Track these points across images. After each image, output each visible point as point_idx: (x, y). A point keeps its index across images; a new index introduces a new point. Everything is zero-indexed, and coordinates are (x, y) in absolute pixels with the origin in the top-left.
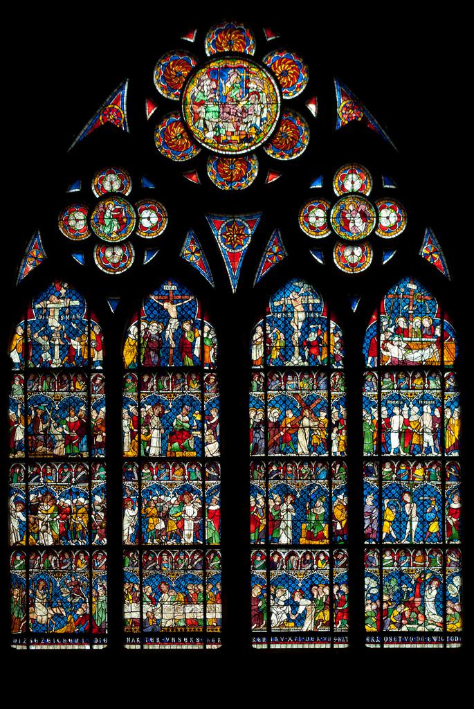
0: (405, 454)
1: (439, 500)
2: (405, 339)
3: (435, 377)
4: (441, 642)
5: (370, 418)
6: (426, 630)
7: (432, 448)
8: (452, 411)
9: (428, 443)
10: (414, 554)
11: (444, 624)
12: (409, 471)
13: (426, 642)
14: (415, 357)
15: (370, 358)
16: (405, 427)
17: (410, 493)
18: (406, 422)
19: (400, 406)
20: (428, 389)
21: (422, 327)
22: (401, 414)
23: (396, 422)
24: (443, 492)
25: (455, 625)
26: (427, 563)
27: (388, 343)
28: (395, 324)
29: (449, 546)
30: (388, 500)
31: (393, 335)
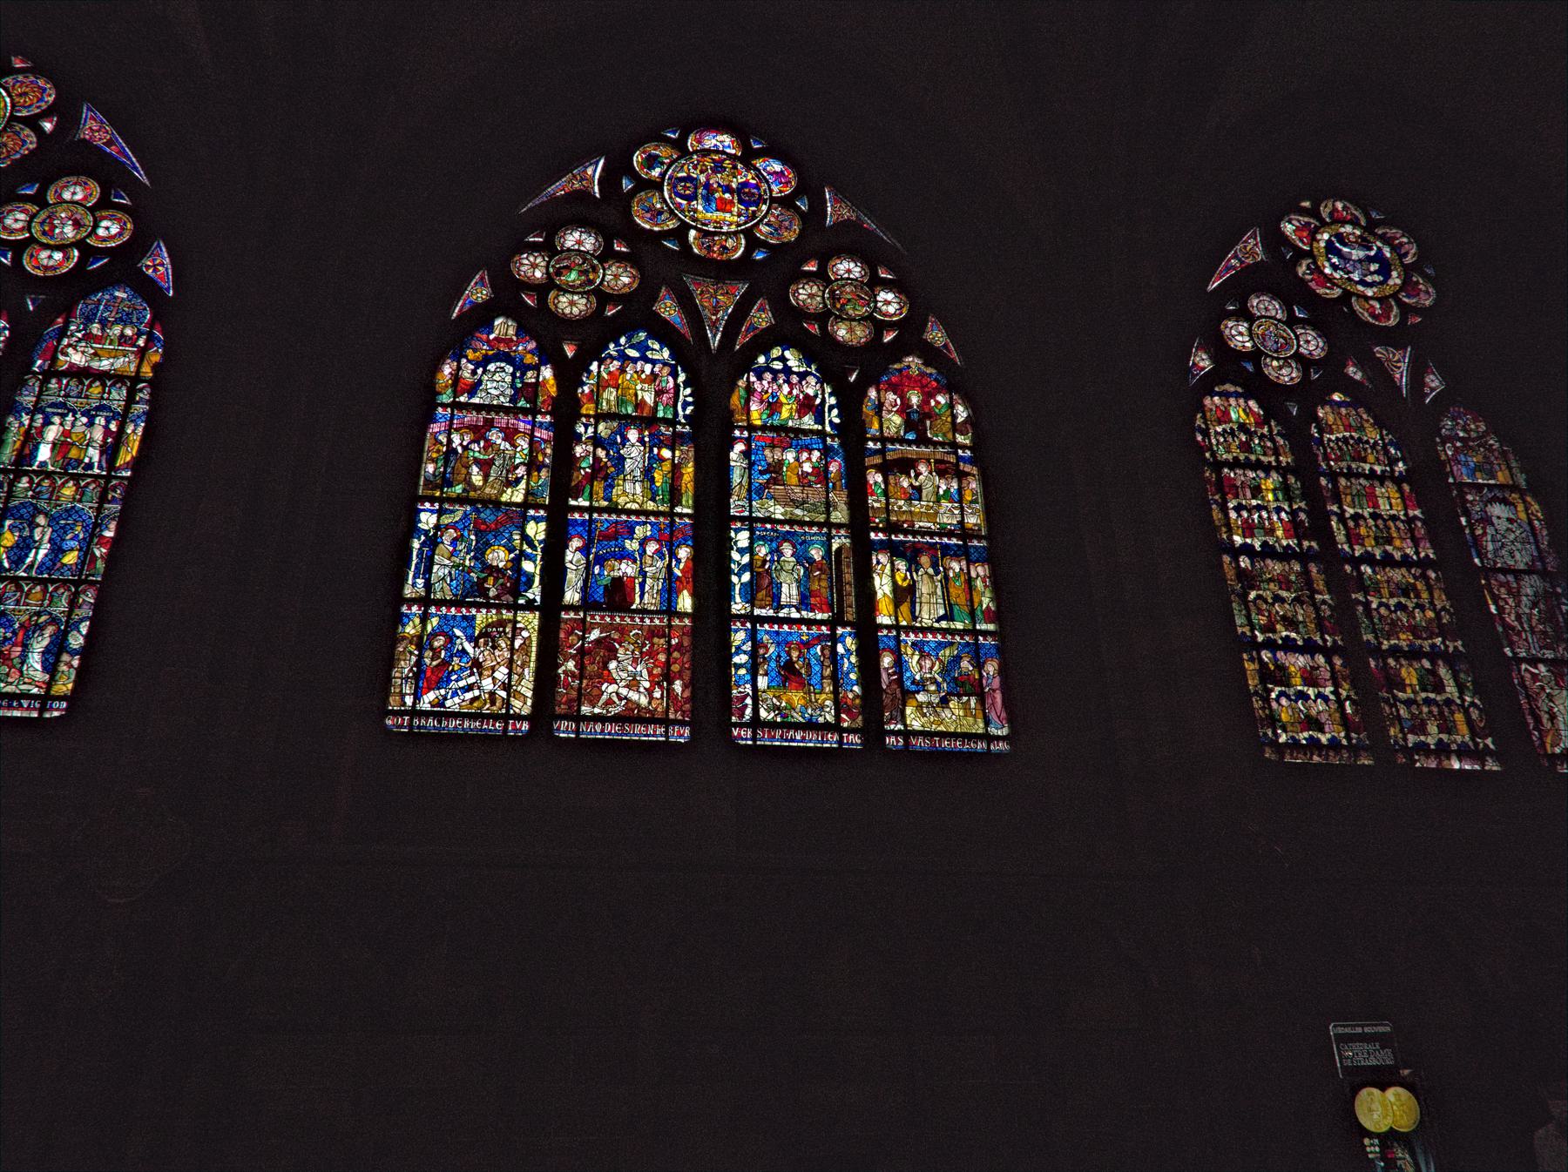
0: (53, 468)
1: (88, 525)
2: (94, 345)
3: (120, 388)
4: (34, 709)
5: (17, 425)
6: (18, 691)
7: (96, 464)
8: (136, 426)
9: (91, 458)
10: (30, 590)
11: (49, 685)
12: (54, 488)
13: (10, 707)
14: (105, 364)
15: (39, 362)
16: (62, 439)
17: (46, 515)
18: (66, 434)
19: (63, 416)
20: (108, 399)
21: (122, 335)
22: (61, 424)
23: (52, 433)
24: (96, 517)
25: (64, 686)
26: (46, 602)
27: (70, 349)
28: (86, 330)
29: (86, 582)
30: (11, 522)
31: (80, 340)
